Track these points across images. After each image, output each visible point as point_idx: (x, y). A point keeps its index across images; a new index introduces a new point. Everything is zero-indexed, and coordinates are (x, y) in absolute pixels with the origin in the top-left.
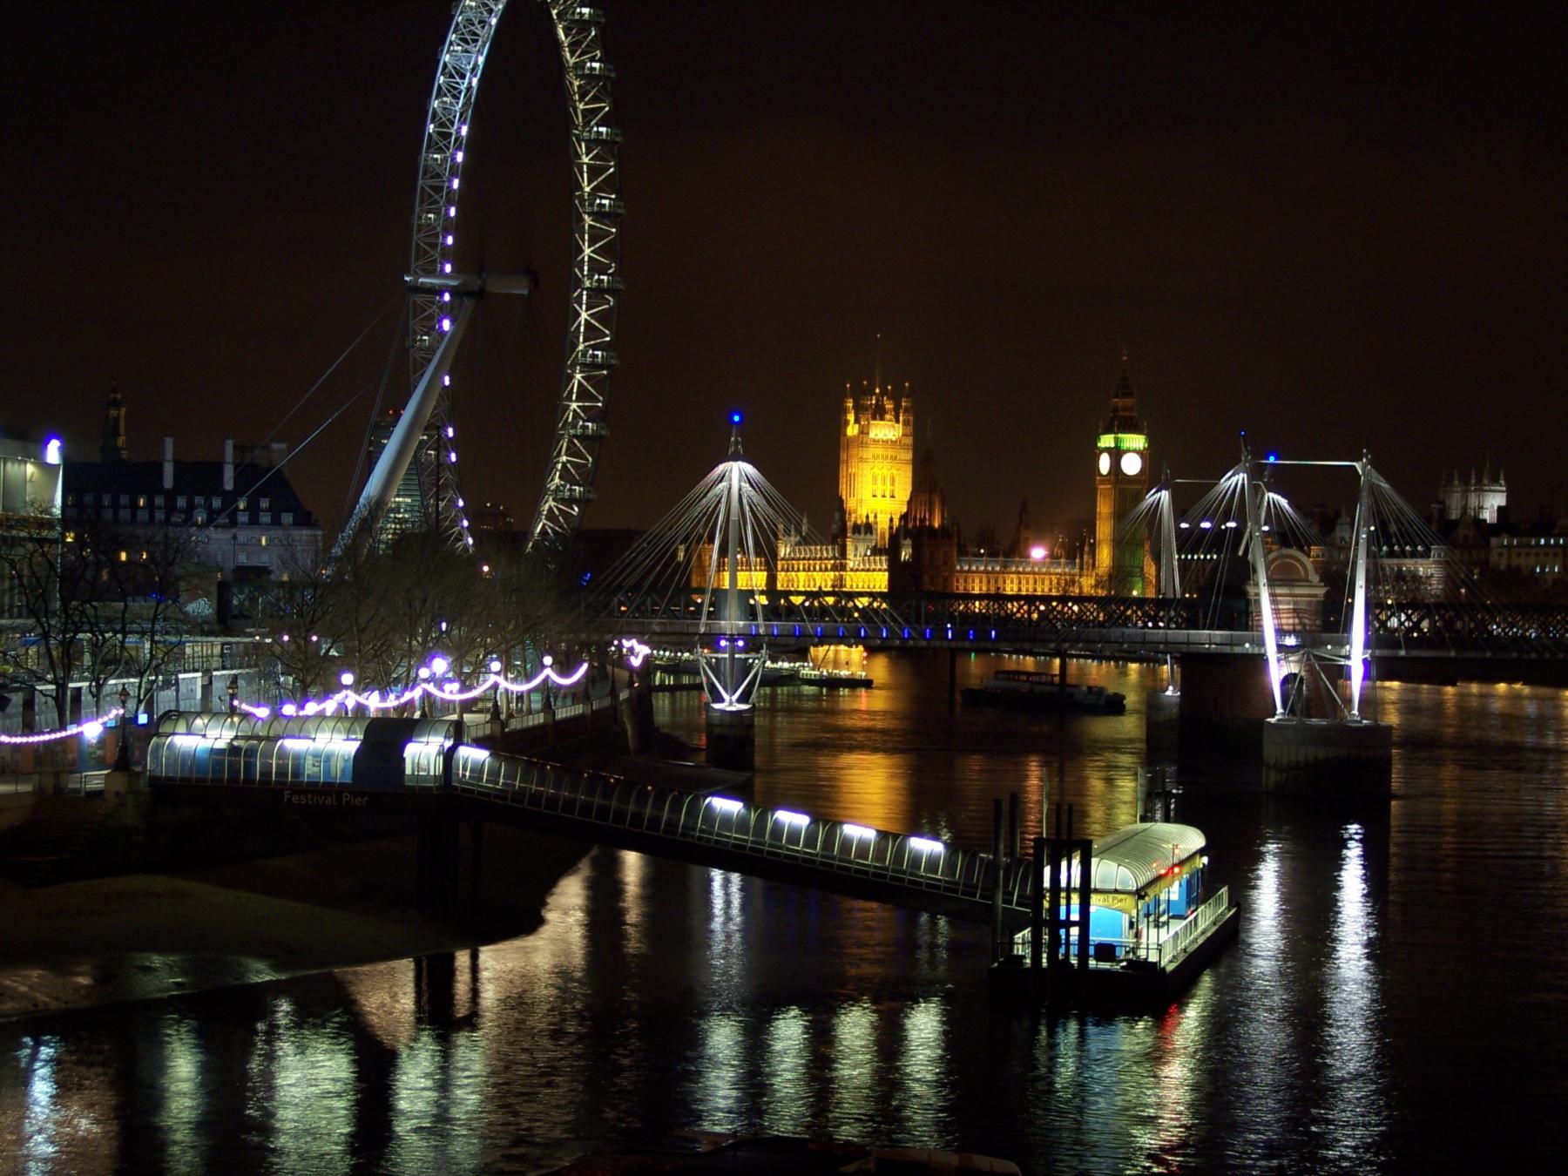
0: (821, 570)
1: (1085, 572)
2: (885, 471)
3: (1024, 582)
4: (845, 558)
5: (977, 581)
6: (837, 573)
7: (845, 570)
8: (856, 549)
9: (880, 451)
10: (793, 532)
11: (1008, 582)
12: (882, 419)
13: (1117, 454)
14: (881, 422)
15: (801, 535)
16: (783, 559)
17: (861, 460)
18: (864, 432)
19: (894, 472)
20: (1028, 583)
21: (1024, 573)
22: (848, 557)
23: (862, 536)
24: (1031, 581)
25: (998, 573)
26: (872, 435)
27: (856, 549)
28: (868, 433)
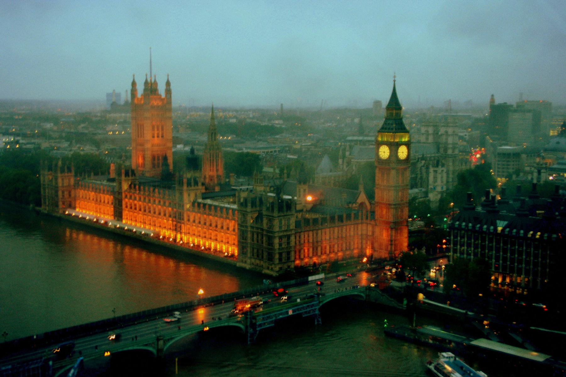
8: (189, 195)
23: (193, 188)
27: (189, 195)
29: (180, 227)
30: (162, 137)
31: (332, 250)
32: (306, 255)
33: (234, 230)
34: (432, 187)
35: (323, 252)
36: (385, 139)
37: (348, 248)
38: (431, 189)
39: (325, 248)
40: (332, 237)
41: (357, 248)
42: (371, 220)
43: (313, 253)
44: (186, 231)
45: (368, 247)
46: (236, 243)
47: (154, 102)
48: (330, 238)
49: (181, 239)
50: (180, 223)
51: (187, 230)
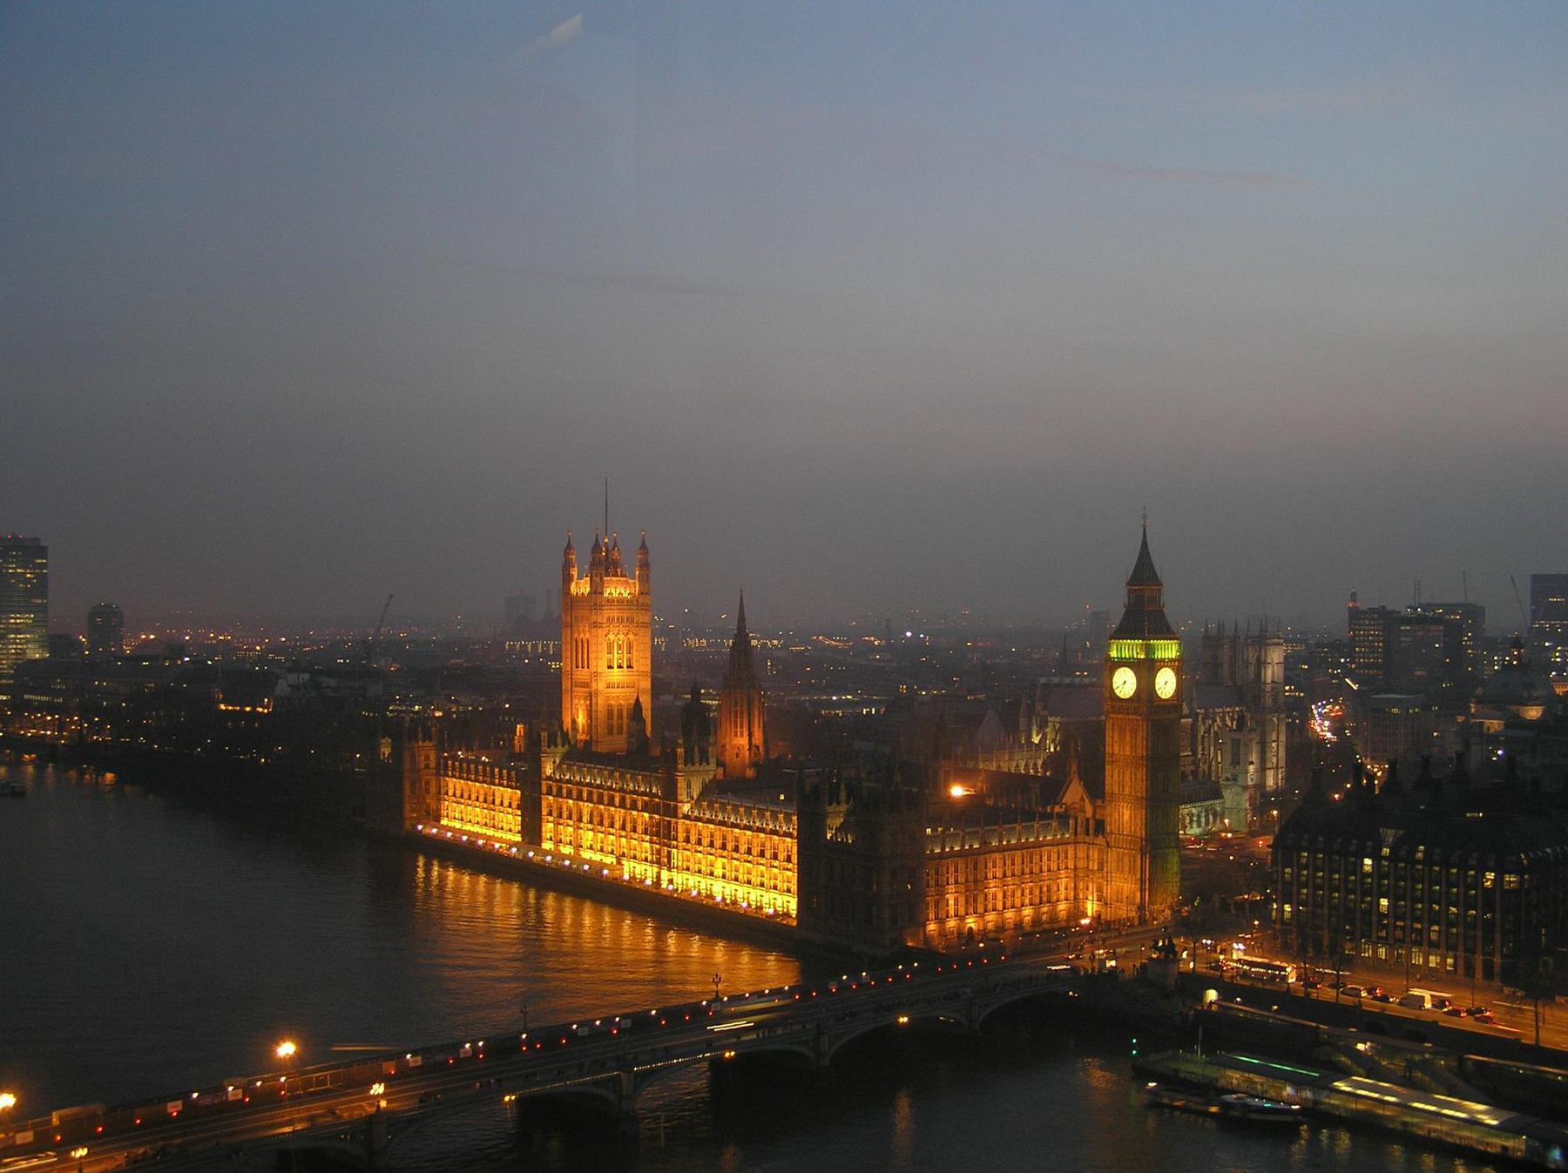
0: (622, 805)
1: (1081, 837)
2: (621, 637)
3: (1009, 862)
4: (676, 800)
5: (952, 869)
6: (657, 817)
7: (676, 816)
8: (689, 786)
9: (615, 614)
10: (559, 741)
11: (990, 865)
12: (616, 575)
13: (1146, 669)
14: (613, 578)
15: (569, 744)
16: (549, 778)
17: (596, 625)
18: (596, 590)
19: (631, 637)
20: (1013, 864)
21: (1009, 848)
22: (679, 798)
24: (1018, 861)
25: (979, 852)
26: (606, 595)
28: (602, 593)
29: (669, 853)
30: (629, 667)
31: (1009, 904)
32: (952, 912)
33: (789, 860)
34: (1229, 776)
35: (990, 907)
36: (1126, 654)
37: (1045, 899)
38: (1228, 779)
39: (995, 898)
40: (1009, 873)
41: (1066, 900)
42: (1096, 835)
43: (967, 909)
44: (680, 863)
45: (1090, 898)
46: (794, 888)
47: (613, 591)
48: (1005, 876)
49: (671, 881)
50: (669, 846)
51: (683, 861)
